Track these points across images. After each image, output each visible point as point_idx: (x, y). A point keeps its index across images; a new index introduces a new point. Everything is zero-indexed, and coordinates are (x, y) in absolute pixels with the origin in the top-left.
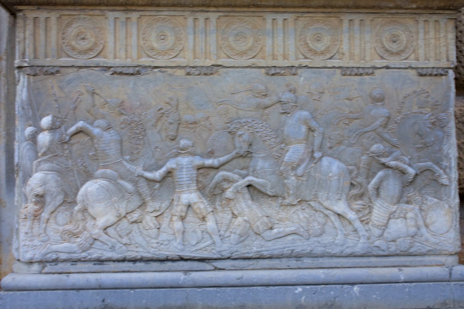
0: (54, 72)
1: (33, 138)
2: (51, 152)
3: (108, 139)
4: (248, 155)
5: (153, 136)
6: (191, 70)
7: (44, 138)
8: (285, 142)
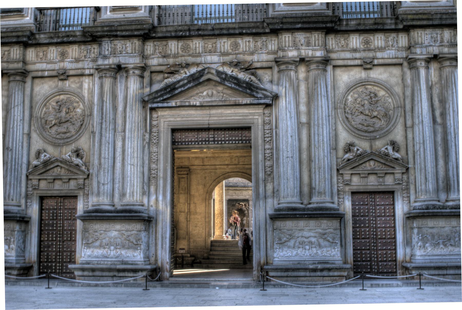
0: (421, 228)
1: (419, 238)
2: (421, 240)
3: (430, 238)
4: (450, 239)
5: (436, 237)
6: (441, 227)
7: (420, 238)
8: (455, 238)
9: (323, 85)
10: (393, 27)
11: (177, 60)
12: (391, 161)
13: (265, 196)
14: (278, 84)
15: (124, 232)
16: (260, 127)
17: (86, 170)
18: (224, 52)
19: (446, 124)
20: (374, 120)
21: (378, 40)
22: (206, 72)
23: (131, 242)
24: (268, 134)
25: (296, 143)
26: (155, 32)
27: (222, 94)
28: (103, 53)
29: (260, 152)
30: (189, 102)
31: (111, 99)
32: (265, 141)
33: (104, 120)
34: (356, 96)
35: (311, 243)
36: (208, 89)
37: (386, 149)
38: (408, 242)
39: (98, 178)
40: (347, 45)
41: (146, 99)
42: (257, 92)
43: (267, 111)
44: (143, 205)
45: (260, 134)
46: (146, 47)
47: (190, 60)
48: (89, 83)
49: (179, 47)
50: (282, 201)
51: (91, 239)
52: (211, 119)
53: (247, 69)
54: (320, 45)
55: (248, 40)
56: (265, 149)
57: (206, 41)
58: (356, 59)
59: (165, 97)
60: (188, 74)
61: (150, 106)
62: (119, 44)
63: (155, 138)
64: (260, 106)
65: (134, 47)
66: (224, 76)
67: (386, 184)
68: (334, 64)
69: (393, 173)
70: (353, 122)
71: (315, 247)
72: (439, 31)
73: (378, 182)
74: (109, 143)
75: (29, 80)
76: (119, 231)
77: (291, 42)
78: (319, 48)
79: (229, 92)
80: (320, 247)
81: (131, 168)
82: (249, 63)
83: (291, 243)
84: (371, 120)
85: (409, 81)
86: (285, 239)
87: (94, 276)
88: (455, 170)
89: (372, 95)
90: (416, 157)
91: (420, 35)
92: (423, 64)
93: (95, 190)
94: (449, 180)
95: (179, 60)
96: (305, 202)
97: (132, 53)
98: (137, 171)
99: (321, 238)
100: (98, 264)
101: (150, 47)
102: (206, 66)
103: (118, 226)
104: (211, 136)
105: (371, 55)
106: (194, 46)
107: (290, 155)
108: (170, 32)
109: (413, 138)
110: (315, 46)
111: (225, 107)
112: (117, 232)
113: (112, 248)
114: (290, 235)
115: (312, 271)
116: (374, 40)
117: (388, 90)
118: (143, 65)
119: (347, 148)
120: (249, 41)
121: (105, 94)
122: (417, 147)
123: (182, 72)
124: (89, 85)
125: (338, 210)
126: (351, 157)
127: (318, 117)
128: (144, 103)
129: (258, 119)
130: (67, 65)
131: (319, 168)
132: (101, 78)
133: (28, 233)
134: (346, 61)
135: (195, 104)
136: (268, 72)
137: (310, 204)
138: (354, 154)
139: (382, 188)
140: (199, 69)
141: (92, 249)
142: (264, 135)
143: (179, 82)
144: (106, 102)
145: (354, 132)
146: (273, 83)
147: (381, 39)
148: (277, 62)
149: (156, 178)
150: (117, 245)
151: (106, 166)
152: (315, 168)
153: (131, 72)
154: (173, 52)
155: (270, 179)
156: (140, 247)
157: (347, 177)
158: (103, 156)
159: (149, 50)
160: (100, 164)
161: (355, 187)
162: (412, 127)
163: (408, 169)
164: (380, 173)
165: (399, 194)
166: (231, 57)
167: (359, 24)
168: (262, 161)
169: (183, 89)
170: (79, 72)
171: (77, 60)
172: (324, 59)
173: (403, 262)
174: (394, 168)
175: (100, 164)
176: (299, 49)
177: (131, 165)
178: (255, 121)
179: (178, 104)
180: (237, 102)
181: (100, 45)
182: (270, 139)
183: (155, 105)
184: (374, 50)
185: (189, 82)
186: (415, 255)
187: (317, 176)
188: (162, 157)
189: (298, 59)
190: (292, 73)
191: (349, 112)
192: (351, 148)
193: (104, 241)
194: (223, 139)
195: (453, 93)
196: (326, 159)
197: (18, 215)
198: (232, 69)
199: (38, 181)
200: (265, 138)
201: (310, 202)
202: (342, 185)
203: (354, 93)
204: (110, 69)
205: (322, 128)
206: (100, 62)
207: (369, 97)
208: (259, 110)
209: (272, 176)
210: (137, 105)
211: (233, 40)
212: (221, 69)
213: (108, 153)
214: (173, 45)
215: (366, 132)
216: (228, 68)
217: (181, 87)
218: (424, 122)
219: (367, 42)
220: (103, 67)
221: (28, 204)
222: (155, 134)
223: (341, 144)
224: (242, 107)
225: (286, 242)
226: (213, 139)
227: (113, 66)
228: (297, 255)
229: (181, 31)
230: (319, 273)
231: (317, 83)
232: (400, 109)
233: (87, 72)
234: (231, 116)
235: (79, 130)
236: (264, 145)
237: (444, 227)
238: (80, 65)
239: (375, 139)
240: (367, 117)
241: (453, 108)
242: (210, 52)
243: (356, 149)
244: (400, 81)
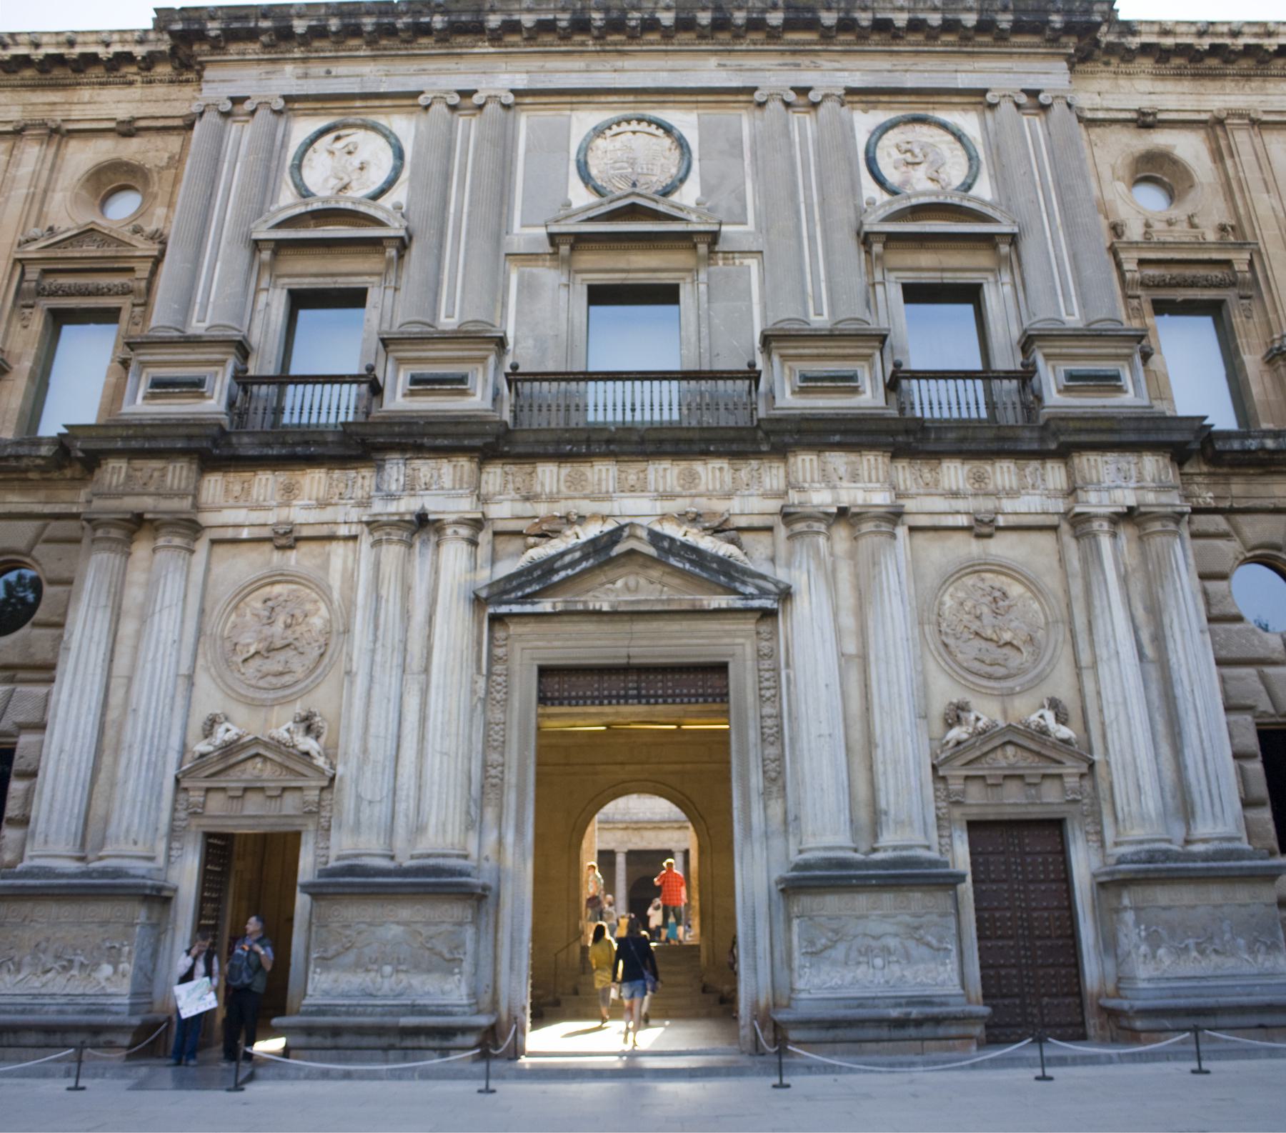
0: (1142, 909)
2: (1147, 938)
3: (1164, 933)
7: (1143, 934)
9: (892, 569)
10: (1035, 446)
11: (556, 506)
12: (1054, 746)
13: (766, 832)
14: (789, 565)
15: (419, 927)
16: (749, 664)
17: (327, 767)
18: (665, 491)
19: (1168, 661)
20: (1007, 650)
21: (1002, 473)
22: (625, 534)
23: (436, 954)
24: (767, 680)
25: (838, 702)
26: (509, 443)
27: (659, 586)
28: (385, 487)
29: (751, 723)
30: (585, 603)
31: (399, 594)
32: (761, 696)
33: (379, 645)
34: (961, 595)
35: (887, 951)
36: (626, 575)
37: (1041, 716)
38: (1109, 944)
39: (357, 786)
40: (937, 482)
41: (484, 594)
42: (744, 583)
43: (765, 628)
44: (466, 857)
45: (750, 680)
46: (484, 476)
47: (586, 507)
48: (346, 557)
49: (562, 478)
50: (810, 842)
51: (334, 947)
52: (633, 643)
53: (716, 531)
54: (881, 479)
55: (718, 466)
56: (762, 717)
57: (624, 466)
58: (958, 513)
59: (528, 590)
60: (583, 539)
61: (491, 610)
62: (424, 468)
63: (499, 688)
64: (749, 615)
65: (458, 474)
66: (666, 544)
67: (1045, 800)
68: (912, 524)
69: (1060, 776)
70: (959, 656)
71: (898, 962)
72: (1132, 458)
73: (1027, 797)
74: (389, 700)
75: (202, 546)
76: (406, 924)
77: (816, 472)
78: (878, 485)
79: (676, 581)
80: (909, 962)
81: (441, 762)
82: (722, 515)
83: (839, 952)
84: (999, 650)
85: (1075, 563)
86: (823, 941)
87: (336, 1048)
88: (1201, 765)
89: (997, 594)
90: (1109, 736)
91: (1092, 463)
92: (1106, 526)
93: (349, 817)
94: (1190, 792)
95: (559, 509)
96: (864, 847)
97: (454, 488)
98: (456, 768)
99: (912, 937)
100: (348, 1014)
101: (494, 476)
102: (623, 521)
103: (406, 912)
104: (630, 685)
106: (596, 477)
107: (825, 730)
108: (544, 443)
109: (1099, 693)
110: (870, 481)
111: (666, 617)
112: (402, 928)
113: (388, 969)
114: (836, 931)
115: (895, 1027)
116: (994, 473)
117: (1032, 583)
118: (480, 516)
119: (952, 714)
120: (721, 469)
121: (386, 582)
122: (1109, 713)
123: (569, 533)
124: (345, 562)
125: (946, 864)
126: (965, 736)
127: (885, 642)
128: (478, 602)
129: (743, 645)
131: (896, 762)
132: (377, 543)
133: (166, 931)
134: (936, 517)
135: (597, 607)
136: (764, 538)
137: (875, 850)
138: (971, 730)
139: (1036, 812)
140: (609, 526)
141: (333, 975)
142: (760, 682)
143: (562, 555)
144: (387, 601)
145: (965, 679)
146: (777, 562)
147: (1009, 471)
148: (788, 516)
149: (499, 787)
150: (400, 964)
151: (380, 758)
152: (884, 763)
153: (449, 531)
154: (547, 490)
155: (775, 789)
156: (460, 966)
157: (956, 785)
158: (372, 730)
159: (491, 482)
160: (365, 751)
161: (975, 810)
162: (1094, 665)
163: (1092, 765)
164: (1031, 776)
165: (1076, 826)
166: (680, 501)
167: (963, 440)
168: (756, 745)
169: (570, 572)
170: (324, 531)
172: (891, 510)
173: (1100, 996)
174: (1060, 762)
175: (365, 751)
176: (834, 487)
177: (442, 753)
178: (738, 650)
179: (560, 607)
180: (698, 603)
181: (380, 468)
182: (773, 692)
183: (504, 609)
184: (996, 494)
185: (585, 557)
186: (1133, 979)
187: (891, 782)
188: (514, 736)
189: (834, 510)
190: (822, 540)
191: (949, 631)
192: (962, 715)
193: (367, 950)
194: (660, 692)
195: (1176, 590)
196: (909, 739)
197: (149, 882)
198: (685, 528)
199: (202, 793)
200: (760, 689)
201: (876, 846)
202: (944, 804)
203: (956, 589)
204: (400, 524)
205: (897, 666)
206: (378, 507)
207: (990, 598)
208: (749, 625)
209: (780, 783)
210: (461, 609)
211: (683, 465)
212: (657, 528)
213: (387, 723)
214: (548, 474)
215: (989, 677)
216: (675, 527)
217: (565, 567)
218: (1121, 656)
219: (979, 478)
220: (385, 518)
221: (174, 853)
222: (499, 679)
223: (938, 707)
224: (708, 616)
225: (826, 948)
226: (635, 692)
227: (407, 518)
228: (855, 982)
229: (569, 442)
230: (912, 1032)
231: (880, 564)
232: (1060, 625)
233: (343, 531)
234: (680, 638)
235: (315, 668)
236: (761, 707)
237: (1194, 907)
238: (328, 514)
239: (1011, 694)
240: (989, 643)
241: (1181, 623)
242: (632, 489)
243: (972, 717)
244: (1056, 564)
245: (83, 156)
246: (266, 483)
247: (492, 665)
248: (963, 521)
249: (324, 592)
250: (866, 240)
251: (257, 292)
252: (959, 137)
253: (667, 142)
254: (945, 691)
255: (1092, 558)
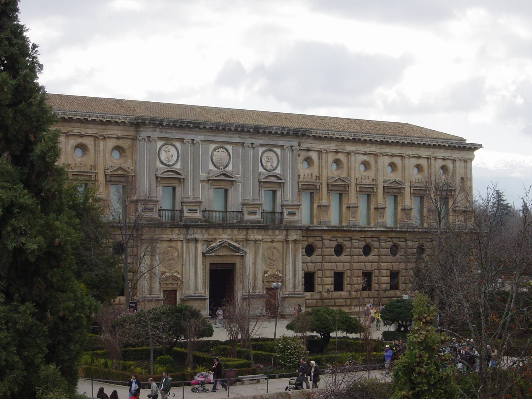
53: (236, 242)
103: (198, 302)
105: (275, 237)
130: (174, 236)
171: (178, 235)
238: (178, 236)
245: (111, 143)
246: (168, 231)
247: (204, 263)
248: (270, 240)
249: (177, 250)
250: (260, 182)
251: (157, 186)
252: (277, 155)
253: (227, 153)
254: (265, 268)
255: (288, 247)
